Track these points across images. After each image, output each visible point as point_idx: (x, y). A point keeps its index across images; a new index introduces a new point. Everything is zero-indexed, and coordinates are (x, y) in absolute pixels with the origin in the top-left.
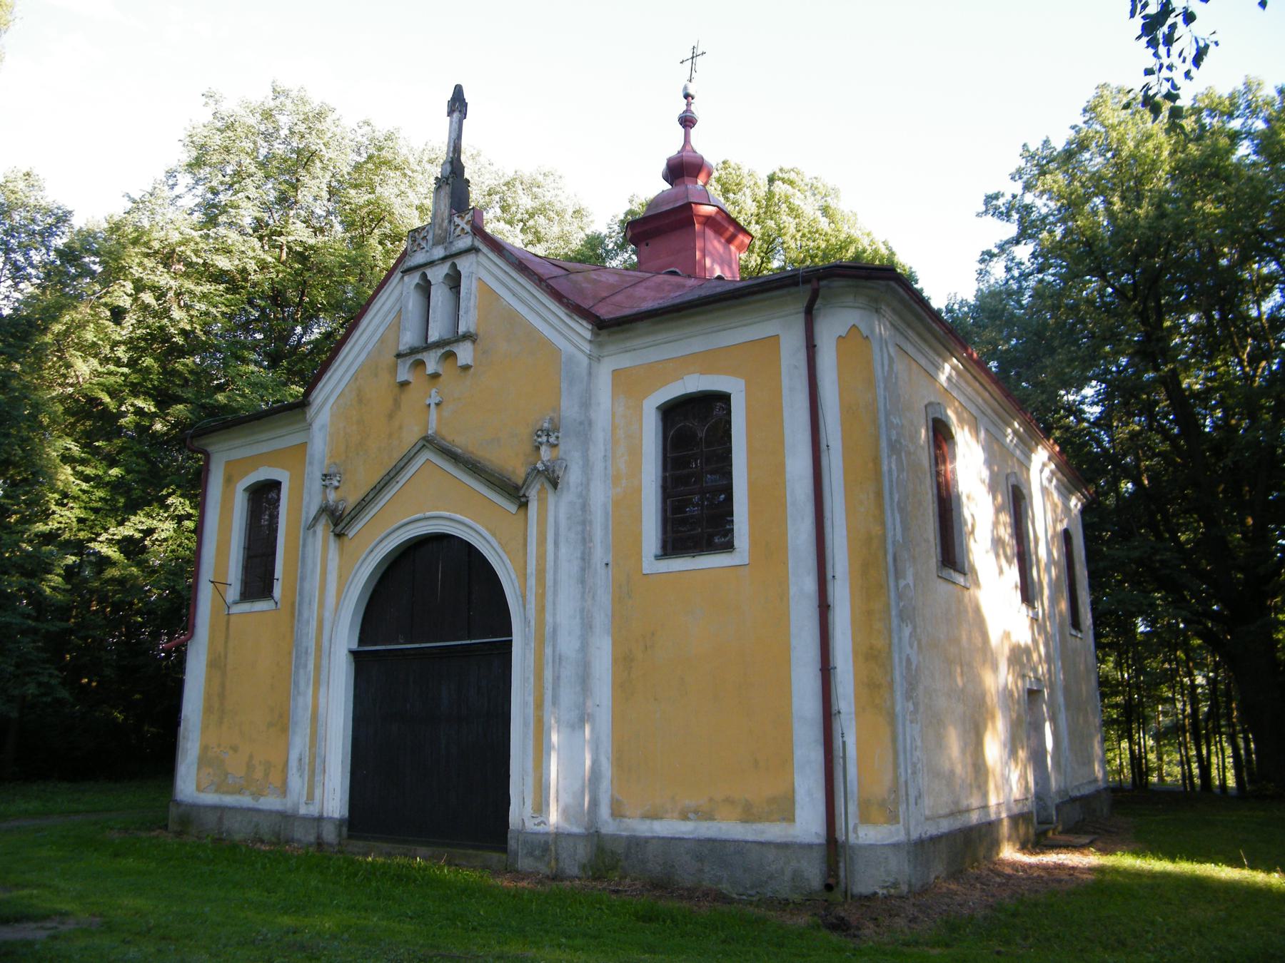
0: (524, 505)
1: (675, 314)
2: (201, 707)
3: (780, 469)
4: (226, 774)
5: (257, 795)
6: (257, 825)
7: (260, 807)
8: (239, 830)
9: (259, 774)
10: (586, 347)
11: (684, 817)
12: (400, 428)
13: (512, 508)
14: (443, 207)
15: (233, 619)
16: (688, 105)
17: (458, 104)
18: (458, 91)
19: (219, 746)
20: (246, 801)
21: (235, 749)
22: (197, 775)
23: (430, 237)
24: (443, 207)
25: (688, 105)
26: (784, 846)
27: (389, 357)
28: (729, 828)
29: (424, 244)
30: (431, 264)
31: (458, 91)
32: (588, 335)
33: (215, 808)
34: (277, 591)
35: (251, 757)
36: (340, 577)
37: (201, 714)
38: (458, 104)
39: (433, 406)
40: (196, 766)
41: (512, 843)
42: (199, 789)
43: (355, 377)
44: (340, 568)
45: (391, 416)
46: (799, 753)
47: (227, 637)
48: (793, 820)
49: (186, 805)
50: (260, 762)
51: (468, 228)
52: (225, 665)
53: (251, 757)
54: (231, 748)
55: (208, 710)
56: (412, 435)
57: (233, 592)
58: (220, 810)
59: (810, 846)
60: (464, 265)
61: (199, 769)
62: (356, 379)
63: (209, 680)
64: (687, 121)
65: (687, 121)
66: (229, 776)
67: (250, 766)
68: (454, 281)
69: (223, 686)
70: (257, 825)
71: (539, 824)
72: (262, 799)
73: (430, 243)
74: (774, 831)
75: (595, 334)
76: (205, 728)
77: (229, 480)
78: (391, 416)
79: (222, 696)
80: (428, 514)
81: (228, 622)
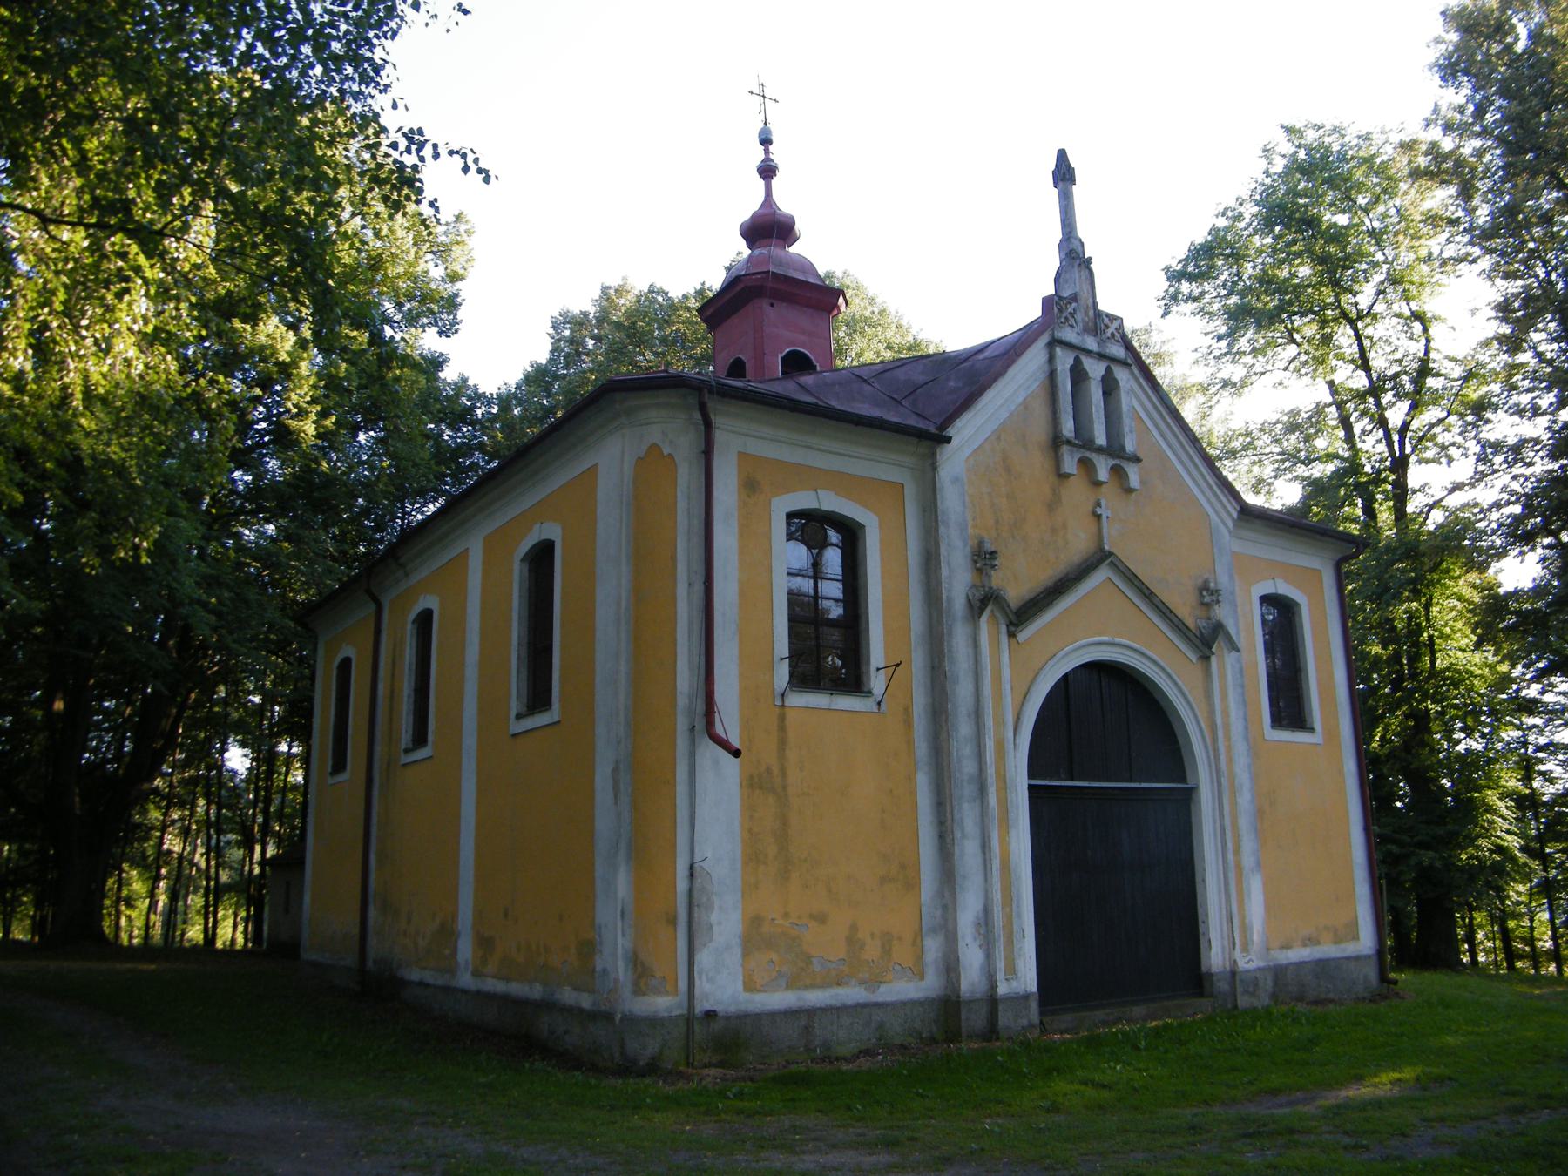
0: (1205, 658)
1: (1318, 537)
2: (739, 852)
3: (1331, 676)
4: (808, 959)
5: (873, 983)
6: (881, 1026)
7: (880, 999)
8: (846, 1036)
9: (872, 951)
10: (1230, 524)
11: (1305, 945)
12: (1064, 526)
13: (1194, 659)
15: (790, 714)
16: (767, 152)
17: (1064, 174)
18: (1062, 155)
19: (786, 915)
20: (852, 994)
21: (821, 919)
22: (742, 966)
23: (1079, 316)
25: (767, 152)
26: (1357, 958)
27: (1039, 430)
28: (1328, 950)
29: (1072, 320)
30: (1088, 352)
31: (1062, 155)
32: (1235, 514)
33: (791, 1014)
34: (877, 683)
35: (854, 928)
37: (739, 865)
38: (1064, 174)
40: (738, 951)
41: (1222, 986)
42: (749, 986)
43: (997, 435)
46: (1358, 889)
47: (783, 742)
48: (1358, 939)
49: (728, 1018)
50: (872, 935)
51: (1118, 336)
52: (785, 788)
53: (854, 928)
54: (812, 917)
55: (753, 857)
56: (1078, 544)
57: (783, 673)
58: (809, 1014)
59: (1368, 957)
60: (1121, 375)
61: (746, 953)
62: (998, 438)
63: (749, 810)
64: (767, 171)
65: (767, 171)
66: (815, 961)
67: (853, 942)
68: (1109, 387)
69: (785, 822)
70: (881, 1026)
71: (1247, 963)
72: (883, 988)
73: (1081, 325)
74: (1350, 949)
75: (1239, 518)
76: (749, 888)
77: (750, 485)
80: (1117, 640)
81: (782, 718)
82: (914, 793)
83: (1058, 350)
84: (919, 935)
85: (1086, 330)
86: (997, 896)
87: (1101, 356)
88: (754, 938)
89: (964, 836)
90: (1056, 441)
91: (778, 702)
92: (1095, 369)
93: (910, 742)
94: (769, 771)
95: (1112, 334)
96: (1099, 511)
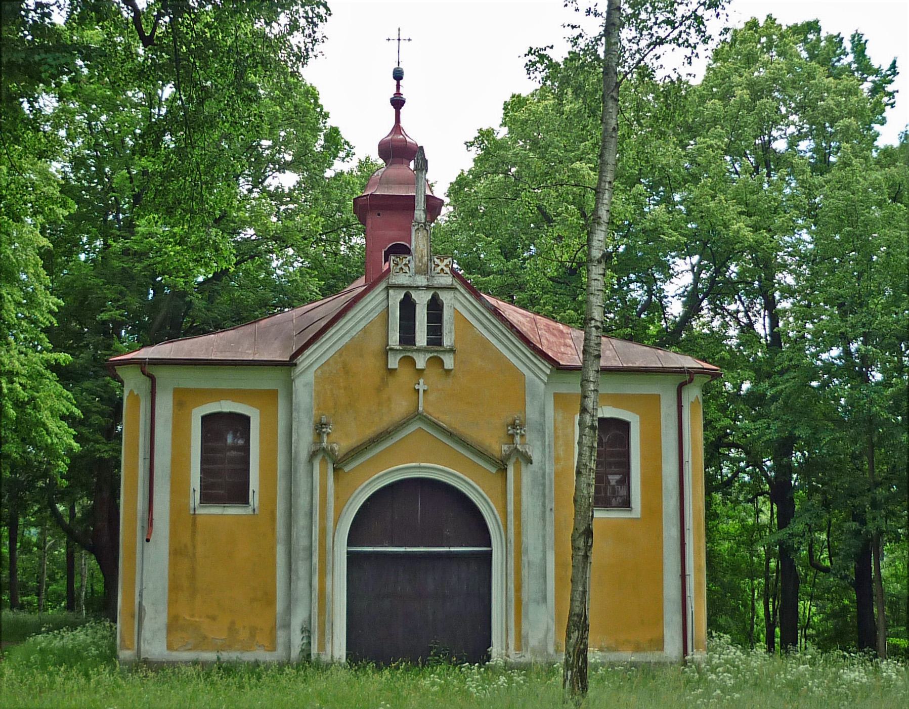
12: (389, 399)
14: (421, 246)
21: (214, 618)
24: (421, 246)
27: (375, 344)
29: (406, 269)
34: (254, 499)
36: (337, 498)
37: (167, 591)
39: (421, 392)
40: (164, 632)
42: (170, 647)
43: (340, 352)
44: (336, 492)
45: (379, 390)
47: (194, 532)
50: (244, 627)
52: (194, 555)
53: (233, 623)
54: (208, 617)
55: (174, 587)
56: (400, 407)
69: (193, 569)
76: (172, 602)
78: (379, 390)
79: (192, 577)
82: (274, 556)
83: (391, 292)
84: (273, 629)
85: (418, 272)
86: (315, 611)
87: (428, 288)
88: (173, 626)
89: (298, 578)
90: (387, 351)
91: (192, 512)
92: (422, 299)
93: (274, 529)
94: (186, 546)
95: (442, 270)
96: (417, 387)
